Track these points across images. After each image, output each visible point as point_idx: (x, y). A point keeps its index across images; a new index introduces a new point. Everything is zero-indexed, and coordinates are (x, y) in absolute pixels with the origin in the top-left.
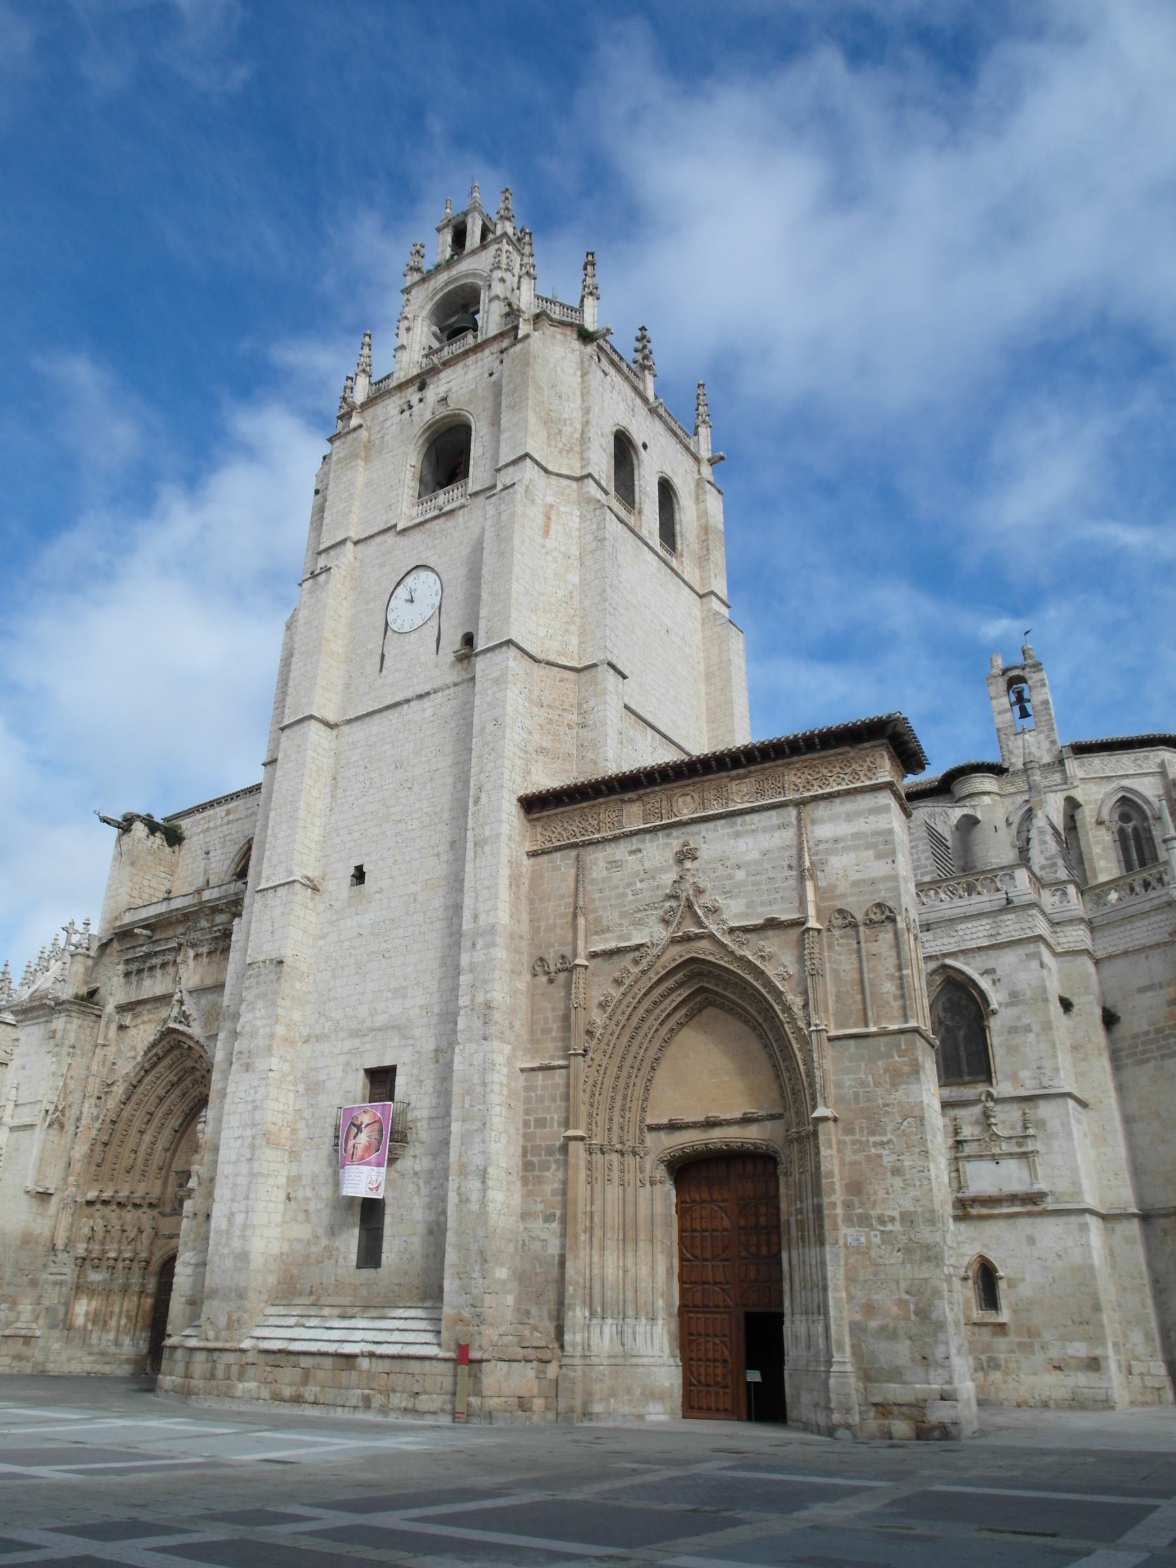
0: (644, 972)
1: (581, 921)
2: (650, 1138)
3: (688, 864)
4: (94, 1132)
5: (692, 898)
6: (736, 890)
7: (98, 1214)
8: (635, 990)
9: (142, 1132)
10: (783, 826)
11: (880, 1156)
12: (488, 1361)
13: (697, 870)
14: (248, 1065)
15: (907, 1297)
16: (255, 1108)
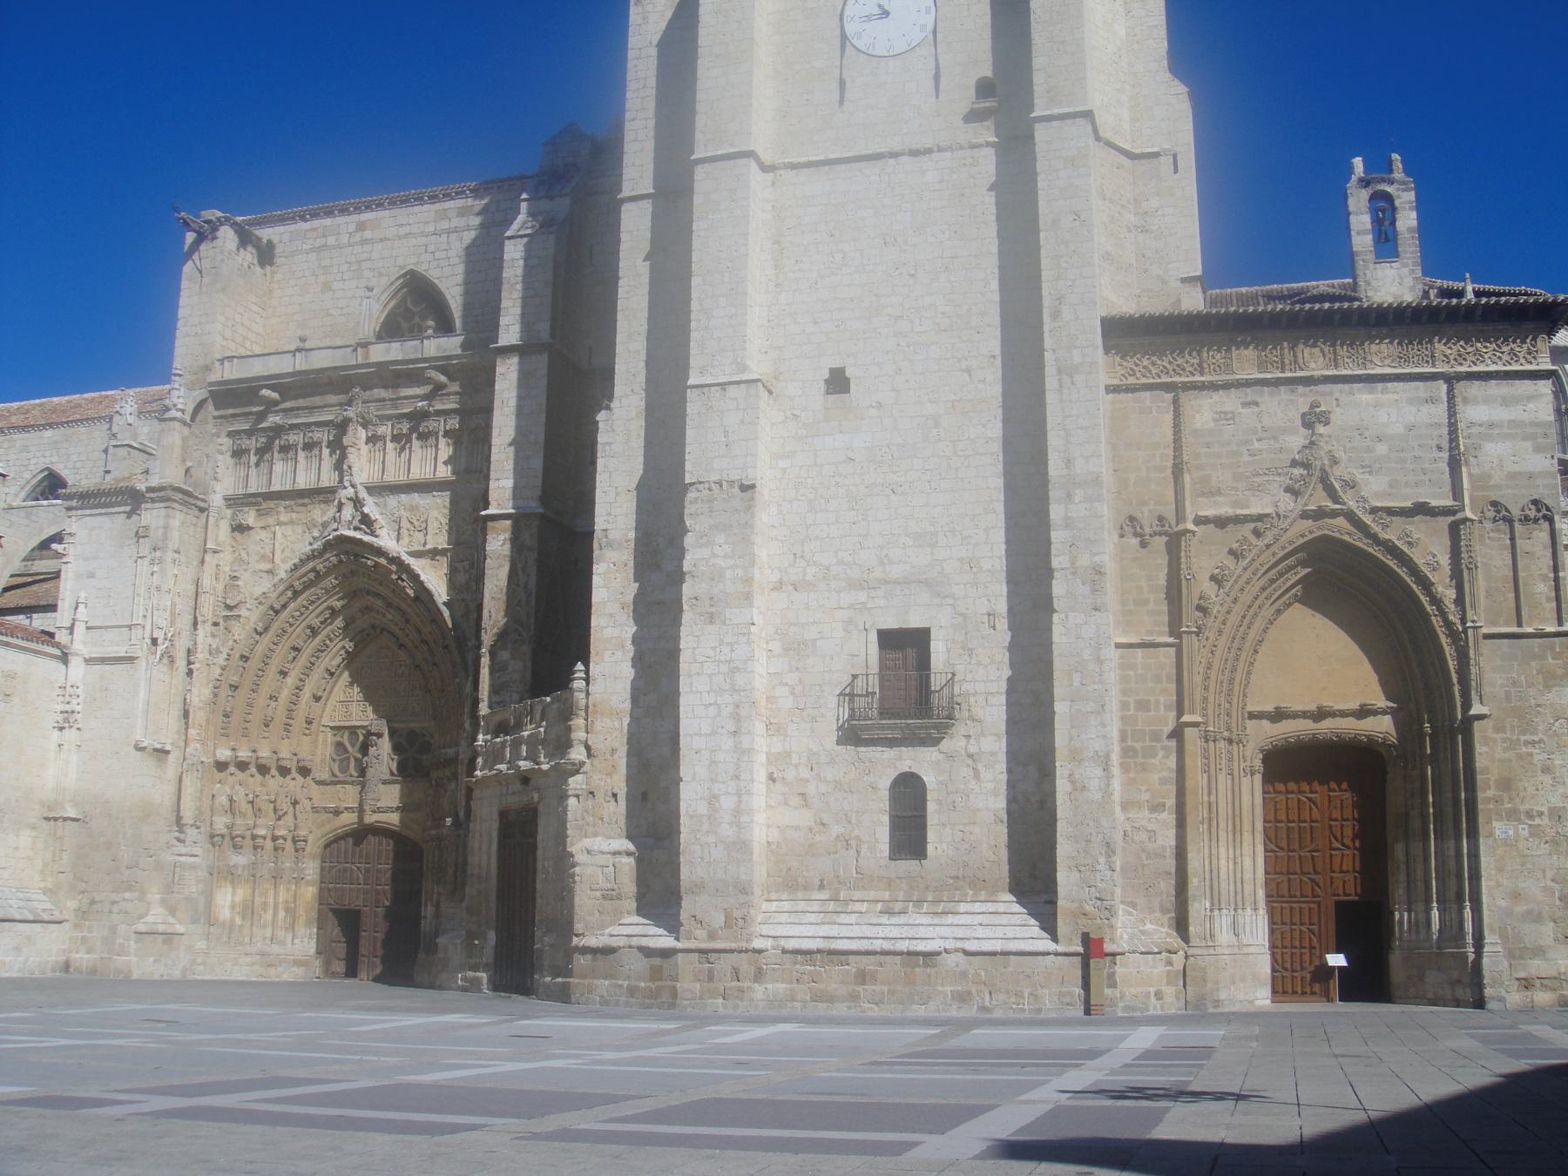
0: (1268, 546)
1: (1187, 478)
2: (1250, 724)
3: (1320, 429)
4: (219, 671)
5: (1327, 468)
6: (1377, 465)
7: (231, 779)
8: (1256, 564)
9: (284, 674)
10: (1432, 400)
11: (1531, 755)
12: (1123, 954)
13: (1330, 436)
14: (711, 616)
15: (1553, 884)
16: (734, 670)
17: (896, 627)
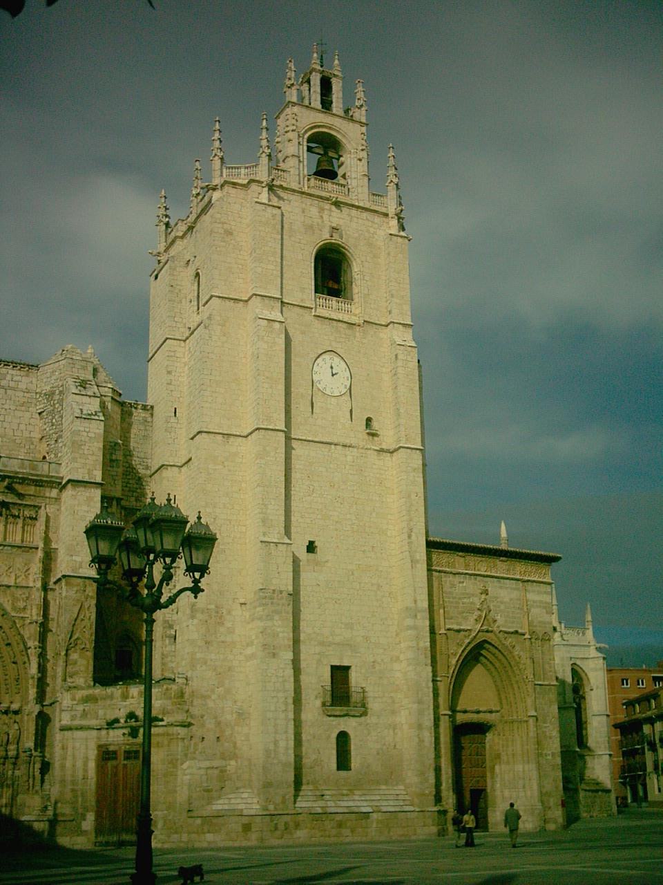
17: (338, 664)
